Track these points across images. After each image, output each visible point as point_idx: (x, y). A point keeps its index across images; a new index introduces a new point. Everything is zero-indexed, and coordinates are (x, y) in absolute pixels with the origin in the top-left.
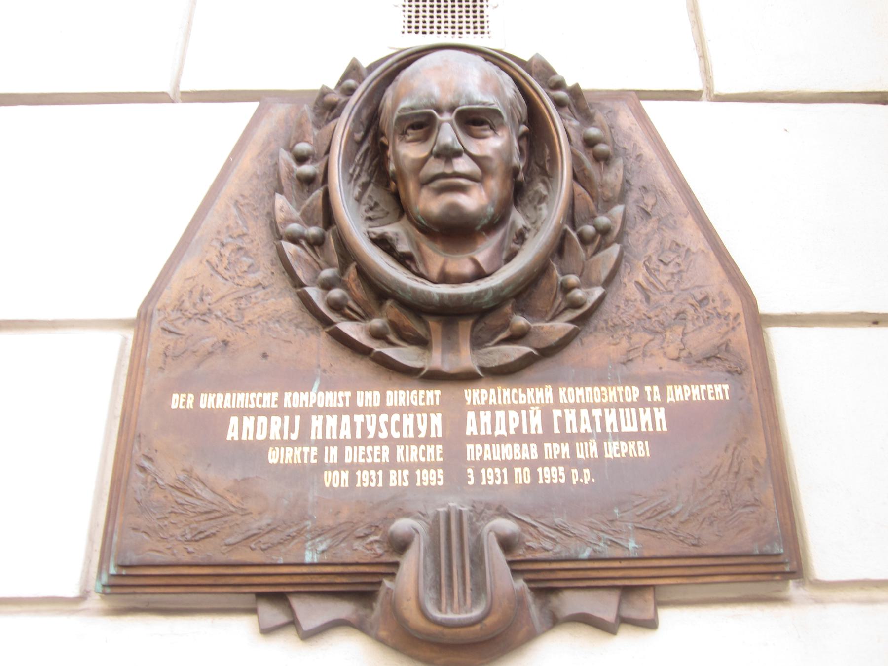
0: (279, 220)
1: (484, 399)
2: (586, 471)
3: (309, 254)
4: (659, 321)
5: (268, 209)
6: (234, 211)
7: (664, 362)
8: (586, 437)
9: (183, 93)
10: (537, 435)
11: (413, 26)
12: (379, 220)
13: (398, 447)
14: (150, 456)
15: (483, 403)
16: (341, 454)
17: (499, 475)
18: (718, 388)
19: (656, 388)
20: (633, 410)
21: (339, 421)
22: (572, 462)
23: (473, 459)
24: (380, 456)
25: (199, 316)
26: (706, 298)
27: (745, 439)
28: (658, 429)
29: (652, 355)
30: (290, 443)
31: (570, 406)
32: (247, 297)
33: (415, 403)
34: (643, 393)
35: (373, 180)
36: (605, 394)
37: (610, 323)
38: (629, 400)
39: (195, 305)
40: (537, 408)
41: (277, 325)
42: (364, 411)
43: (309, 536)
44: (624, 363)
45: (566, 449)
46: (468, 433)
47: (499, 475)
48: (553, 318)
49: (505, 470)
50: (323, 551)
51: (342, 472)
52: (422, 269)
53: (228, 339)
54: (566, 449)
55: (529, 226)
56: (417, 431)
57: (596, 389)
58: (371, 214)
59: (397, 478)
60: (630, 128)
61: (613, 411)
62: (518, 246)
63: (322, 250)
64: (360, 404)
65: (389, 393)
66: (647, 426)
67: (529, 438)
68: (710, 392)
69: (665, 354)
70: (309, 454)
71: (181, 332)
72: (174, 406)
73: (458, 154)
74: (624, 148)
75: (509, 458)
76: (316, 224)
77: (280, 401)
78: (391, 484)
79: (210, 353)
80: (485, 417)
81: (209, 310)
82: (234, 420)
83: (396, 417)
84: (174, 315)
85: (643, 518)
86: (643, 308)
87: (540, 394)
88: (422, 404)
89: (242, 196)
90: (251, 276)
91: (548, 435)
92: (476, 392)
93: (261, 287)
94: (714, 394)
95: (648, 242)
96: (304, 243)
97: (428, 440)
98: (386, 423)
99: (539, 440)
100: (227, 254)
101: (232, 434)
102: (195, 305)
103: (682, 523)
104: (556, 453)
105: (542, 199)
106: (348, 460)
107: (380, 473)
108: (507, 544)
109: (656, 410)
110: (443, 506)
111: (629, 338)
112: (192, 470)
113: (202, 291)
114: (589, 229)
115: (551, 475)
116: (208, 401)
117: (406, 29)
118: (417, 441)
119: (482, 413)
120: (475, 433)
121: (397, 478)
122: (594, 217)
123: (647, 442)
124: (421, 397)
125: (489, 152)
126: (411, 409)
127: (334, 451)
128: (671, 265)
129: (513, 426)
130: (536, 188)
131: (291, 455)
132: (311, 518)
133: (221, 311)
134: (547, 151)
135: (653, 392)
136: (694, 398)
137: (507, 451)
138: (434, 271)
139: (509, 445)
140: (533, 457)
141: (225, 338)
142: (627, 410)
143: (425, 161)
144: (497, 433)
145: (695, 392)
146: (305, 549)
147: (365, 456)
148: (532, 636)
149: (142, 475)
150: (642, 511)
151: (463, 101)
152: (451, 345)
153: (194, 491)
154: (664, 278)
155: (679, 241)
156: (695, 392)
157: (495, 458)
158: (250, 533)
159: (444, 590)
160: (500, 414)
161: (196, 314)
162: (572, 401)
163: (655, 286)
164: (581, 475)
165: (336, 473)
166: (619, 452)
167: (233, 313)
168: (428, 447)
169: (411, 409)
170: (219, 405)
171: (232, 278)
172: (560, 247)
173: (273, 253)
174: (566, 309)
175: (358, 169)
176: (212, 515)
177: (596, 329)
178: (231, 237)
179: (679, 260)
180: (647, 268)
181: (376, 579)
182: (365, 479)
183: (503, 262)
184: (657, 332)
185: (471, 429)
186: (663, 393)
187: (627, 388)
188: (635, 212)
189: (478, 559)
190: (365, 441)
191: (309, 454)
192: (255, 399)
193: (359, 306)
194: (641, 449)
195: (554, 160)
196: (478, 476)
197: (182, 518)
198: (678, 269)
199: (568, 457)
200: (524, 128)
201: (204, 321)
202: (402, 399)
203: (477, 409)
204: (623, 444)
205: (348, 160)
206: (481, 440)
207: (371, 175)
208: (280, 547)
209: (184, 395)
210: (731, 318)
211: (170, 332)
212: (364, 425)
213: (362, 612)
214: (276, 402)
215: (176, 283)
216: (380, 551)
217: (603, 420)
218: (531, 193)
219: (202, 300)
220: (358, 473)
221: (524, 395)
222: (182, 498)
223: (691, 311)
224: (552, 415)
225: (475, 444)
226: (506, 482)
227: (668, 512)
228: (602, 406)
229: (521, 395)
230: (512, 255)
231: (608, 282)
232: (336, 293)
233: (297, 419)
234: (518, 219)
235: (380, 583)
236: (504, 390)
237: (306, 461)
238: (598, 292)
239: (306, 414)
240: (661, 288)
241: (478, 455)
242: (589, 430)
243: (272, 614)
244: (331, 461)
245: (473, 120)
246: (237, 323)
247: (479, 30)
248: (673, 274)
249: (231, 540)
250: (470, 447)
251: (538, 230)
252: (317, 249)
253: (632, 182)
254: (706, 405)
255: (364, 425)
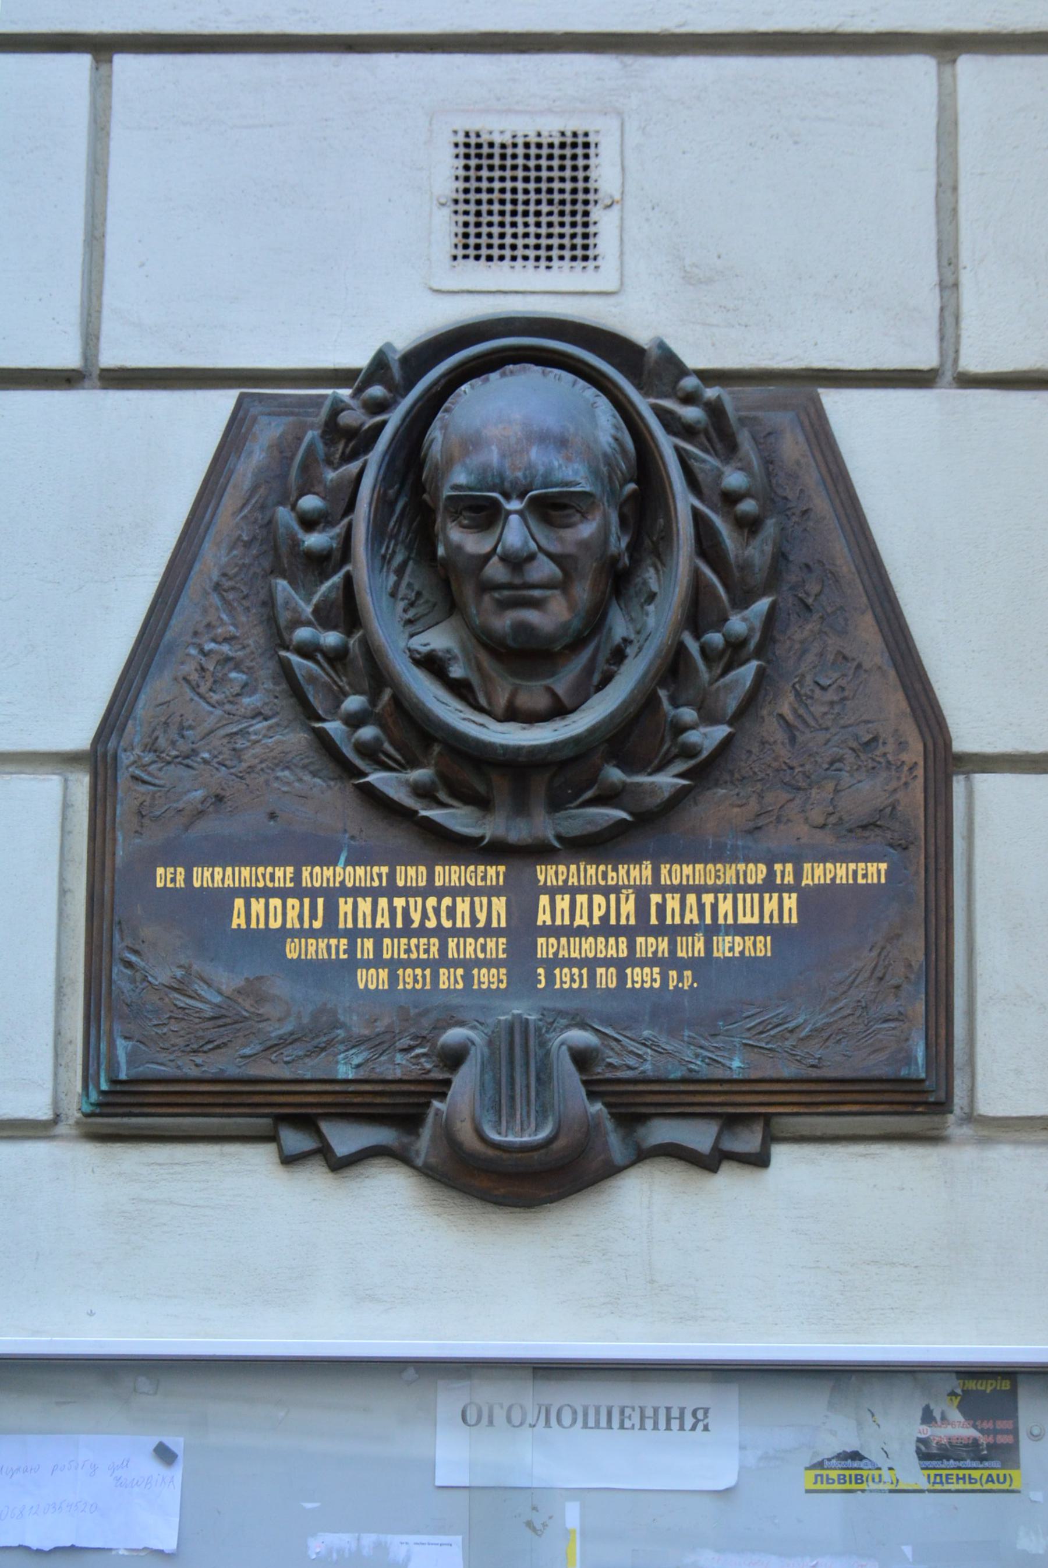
0: (282, 623)
1: (561, 878)
2: (688, 973)
3: (328, 674)
4: (804, 773)
5: (263, 595)
6: (215, 599)
7: (802, 829)
8: (689, 930)
9: (103, 370)
10: (627, 926)
11: (475, 244)
12: (422, 621)
13: (450, 940)
14: (137, 947)
15: (560, 883)
16: (378, 948)
17: (576, 977)
18: (872, 868)
19: (789, 867)
20: (756, 896)
21: (375, 905)
22: (669, 963)
23: (545, 956)
24: (427, 951)
25: (179, 759)
26: (875, 739)
27: (898, 936)
28: (786, 920)
29: (789, 820)
30: (312, 933)
31: (673, 889)
32: (243, 733)
33: (472, 883)
34: (771, 873)
35: (413, 555)
36: (721, 874)
37: (737, 776)
38: (750, 882)
39: (173, 743)
40: (630, 891)
41: (287, 773)
42: (407, 892)
43: (342, 1047)
44: (750, 832)
45: (664, 944)
46: (540, 923)
47: (576, 977)
48: (659, 769)
49: (585, 971)
50: (358, 1066)
51: (380, 971)
52: (483, 701)
53: (223, 793)
54: (664, 944)
55: (632, 636)
56: (474, 920)
57: (710, 866)
58: (410, 615)
59: (449, 978)
60: (798, 463)
61: (730, 896)
62: (614, 668)
63: (345, 665)
64: (400, 883)
65: (439, 869)
66: (771, 917)
67: (617, 931)
68: (860, 873)
69: (806, 819)
70: (337, 947)
71: (157, 782)
72: (160, 884)
73: (531, 557)
74: (786, 498)
75: (591, 955)
76: (334, 628)
77: (297, 878)
78: (442, 986)
79: (201, 813)
80: (563, 903)
81: (193, 750)
82: (239, 903)
83: (447, 901)
84: (148, 758)
85: (754, 1032)
86: (784, 752)
87: (635, 873)
88: (480, 883)
89: (224, 575)
90: (246, 700)
91: (643, 927)
92: (551, 870)
93: (260, 718)
94: (865, 876)
95: (804, 652)
96: (319, 657)
97: (488, 931)
98: (433, 907)
99: (630, 933)
100: (212, 669)
101: (238, 921)
102: (173, 743)
103: (802, 1039)
104: (651, 950)
105: (652, 597)
106: (386, 956)
107: (428, 972)
108: (582, 1059)
109: (785, 895)
110: (504, 1014)
111: (761, 796)
112: (190, 967)
113: (181, 723)
114: (716, 638)
115: (640, 977)
116: (206, 877)
117: (460, 252)
118: (474, 932)
119: (558, 897)
120: (549, 923)
121: (449, 978)
122: (726, 620)
123: (769, 938)
124: (480, 875)
125: (570, 549)
126: (466, 891)
127: (369, 944)
128: (831, 690)
129: (597, 914)
130: (647, 575)
131: (316, 949)
132: (343, 1025)
133: (209, 752)
134: (661, 521)
135: (785, 872)
136: (838, 881)
137: (588, 947)
138: (501, 701)
139: (591, 939)
140: (621, 955)
141: (219, 791)
142: (748, 896)
143: (487, 558)
144: (576, 924)
145: (842, 872)
146: (337, 1062)
147: (408, 951)
148: (611, 1171)
149: (128, 972)
150: (753, 1024)
151: (538, 480)
152: (521, 807)
153: (195, 991)
154: (818, 709)
155: (846, 652)
156: (842, 872)
157: (573, 955)
158: (269, 1043)
159: (504, 1112)
160: (582, 899)
161: (177, 757)
162: (676, 882)
163: (805, 722)
164: (680, 979)
165: (372, 971)
166: (731, 949)
167: (227, 754)
168: (488, 940)
169: (466, 891)
170: (218, 883)
171: (220, 704)
172: (674, 668)
173: (272, 665)
174: (676, 757)
175: (393, 542)
176: (220, 1022)
177: (717, 784)
178: (214, 640)
179: (842, 682)
180: (798, 694)
181: (422, 1100)
182: (408, 978)
183: (592, 689)
184: (799, 789)
185: (543, 918)
186: (798, 874)
187: (751, 866)
188: (790, 605)
189: (544, 1077)
190: (407, 931)
191: (337, 947)
192: (264, 876)
193: (397, 749)
194: (761, 947)
195: (668, 536)
196: (550, 978)
197: (183, 1024)
198: (841, 695)
199: (666, 955)
200: (632, 486)
201: (188, 766)
202: (455, 877)
203: (553, 892)
204: (738, 939)
205: (378, 533)
206: (554, 931)
207: (409, 548)
208: (307, 1060)
209: (172, 870)
210: (906, 768)
211: (144, 782)
212: (406, 910)
213: (406, 1140)
214: (292, 880)
215: (143, 708)
216: (428, 1066)
217: (715, 907)
218: (639, 580)
219: (183, 737)
220: (400, 972)
221: (614, 874)
222: (182, 1001)
223: (850, 757)
224: (649, 900)
225: (548, 937)
226: (585, 986)
227: (786, 1026)
228: (715, 890)
229: (611, 874)
230: (606, 680)
231: (734, 720)
232: (367, 733)
233: (320, 901)
234: (619, 627)
235: (428, 1105)
236: (588, 867)
237: (333, 957)
238: (721, 731)
239: (332, 895)
240: (812, 723)
241: (551, 951)
242: (696, 921)
243: (295, 1140)
244: (366, 957)
245: (552, 507)
246: (232, 770)
247: (579, 253)
248: (832, 703)
249: (247, 1051)
250: (541, 941)
251: (640, 649)
252: (339, 667)
253: (791, 558)
254: (855, 889)
255: (406, 910)
